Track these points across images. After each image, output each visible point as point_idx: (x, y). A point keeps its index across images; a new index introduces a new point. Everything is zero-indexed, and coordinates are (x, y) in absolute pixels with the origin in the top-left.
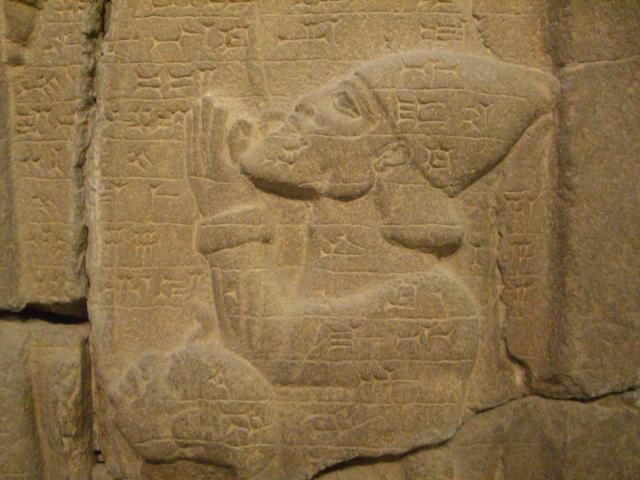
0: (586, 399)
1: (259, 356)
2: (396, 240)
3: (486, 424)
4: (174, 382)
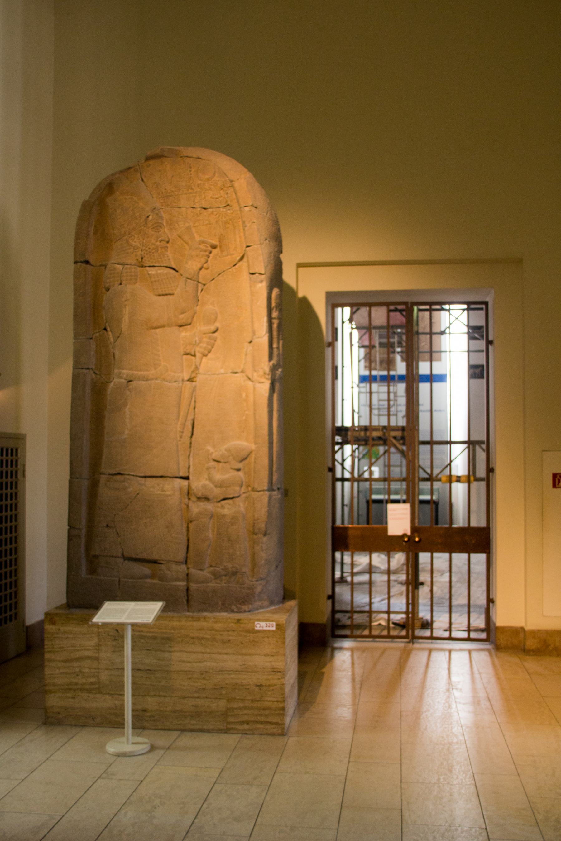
0: (259, 491)
1: (213, 483)
2: (232, 469)
3: (244, 495)
4: (202, 487)
